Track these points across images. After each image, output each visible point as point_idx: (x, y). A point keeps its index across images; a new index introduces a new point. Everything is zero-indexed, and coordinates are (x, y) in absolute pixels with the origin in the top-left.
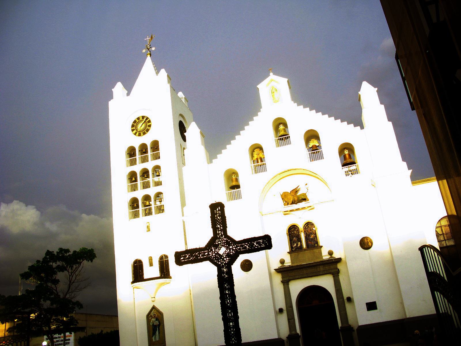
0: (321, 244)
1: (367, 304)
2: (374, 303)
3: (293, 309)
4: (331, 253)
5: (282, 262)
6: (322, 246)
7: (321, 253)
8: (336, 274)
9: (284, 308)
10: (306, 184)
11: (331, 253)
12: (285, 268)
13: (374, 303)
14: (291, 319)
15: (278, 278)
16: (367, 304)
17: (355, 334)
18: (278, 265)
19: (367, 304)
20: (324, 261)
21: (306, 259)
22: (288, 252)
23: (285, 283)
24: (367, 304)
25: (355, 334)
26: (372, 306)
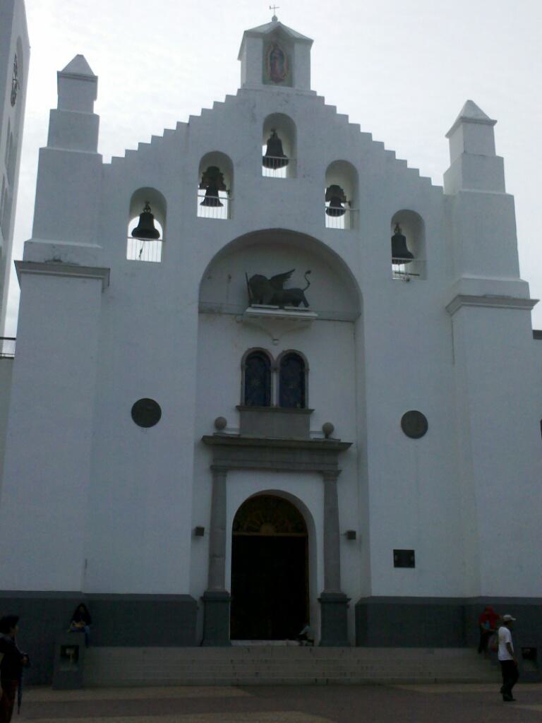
0: (311, 404)
1: (395, 551)
2: (411, 553)
3: (225, 533)
4: (328, 430)
5: (220, 424)
6: (313, 410)
7: (308, 426)
8: (330, 477)
9: (206, 526)
10: (309, 272)
11: (328, 430)
12: (223, 438)
13: (411, 553)
14: (214, 557)
15: (206, 459)
16: (397, 553)
17: (351, 613)
18: (210, 431)
19: (395, 551)
20: (310, 442)
21: (274, 427)
22: (237, 407)
23: (219, 472)
24: (397, 553)
25: (351, 613)
26: (404, 559)
